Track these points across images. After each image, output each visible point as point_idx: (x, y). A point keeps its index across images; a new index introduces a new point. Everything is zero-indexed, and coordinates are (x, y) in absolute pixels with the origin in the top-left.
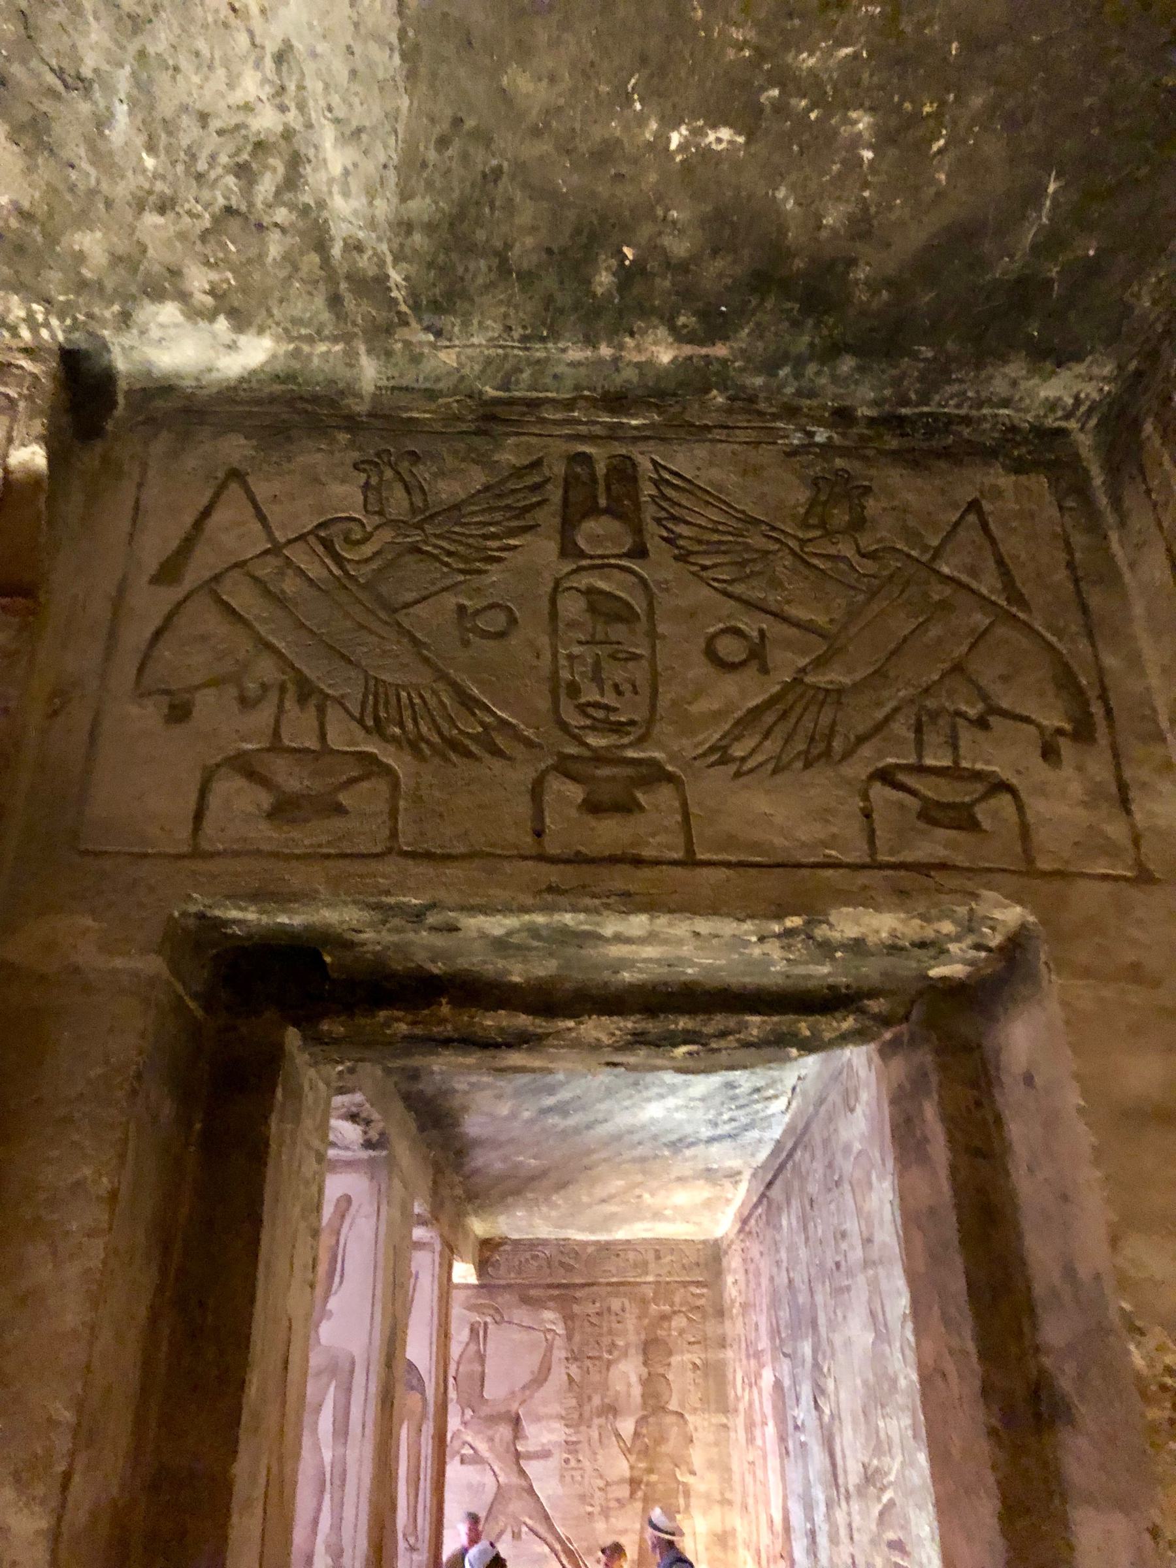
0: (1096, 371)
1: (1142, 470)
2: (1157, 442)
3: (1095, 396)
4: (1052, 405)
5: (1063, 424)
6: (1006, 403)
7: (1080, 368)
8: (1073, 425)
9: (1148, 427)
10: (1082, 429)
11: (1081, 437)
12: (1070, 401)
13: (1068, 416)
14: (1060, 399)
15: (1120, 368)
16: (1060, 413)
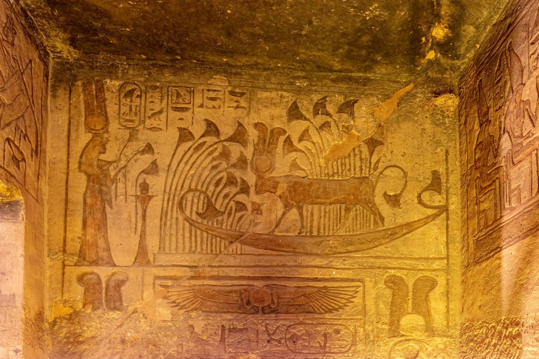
0: (73, 53)
1: (70, 92)
2: (81, 89)
3: (65, 56)
4: (54, 47)
5: (50, 52)
6: (48, 36)
7: (71, 49)
8: (51, 55)
9: (79, 83)
10: (53, 58)
11: (51, 60)
12: (58, 50)
13: (52, 52)
14: (57, 48)
15: (78, 59)
16: (52, 50)
